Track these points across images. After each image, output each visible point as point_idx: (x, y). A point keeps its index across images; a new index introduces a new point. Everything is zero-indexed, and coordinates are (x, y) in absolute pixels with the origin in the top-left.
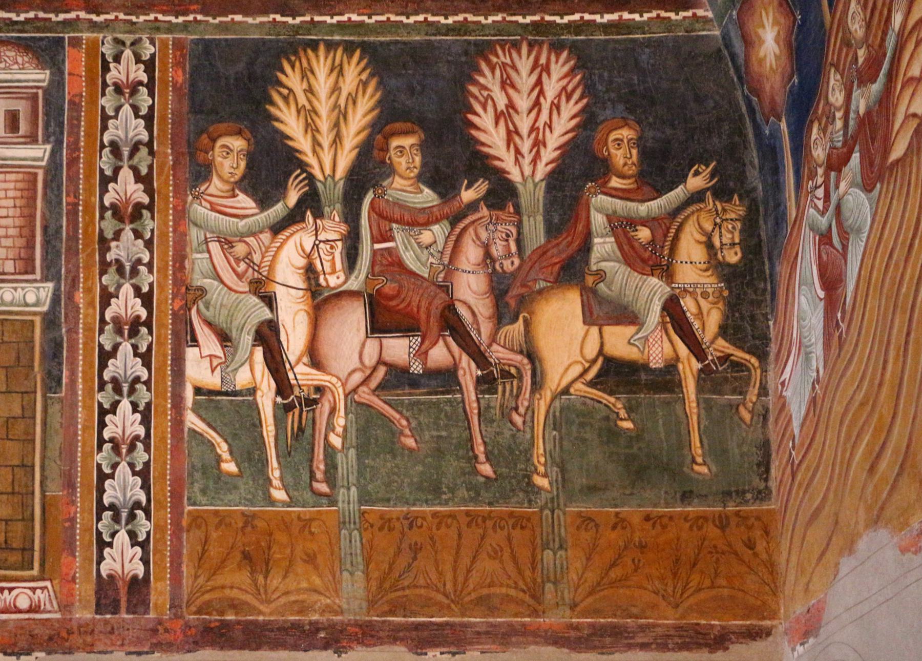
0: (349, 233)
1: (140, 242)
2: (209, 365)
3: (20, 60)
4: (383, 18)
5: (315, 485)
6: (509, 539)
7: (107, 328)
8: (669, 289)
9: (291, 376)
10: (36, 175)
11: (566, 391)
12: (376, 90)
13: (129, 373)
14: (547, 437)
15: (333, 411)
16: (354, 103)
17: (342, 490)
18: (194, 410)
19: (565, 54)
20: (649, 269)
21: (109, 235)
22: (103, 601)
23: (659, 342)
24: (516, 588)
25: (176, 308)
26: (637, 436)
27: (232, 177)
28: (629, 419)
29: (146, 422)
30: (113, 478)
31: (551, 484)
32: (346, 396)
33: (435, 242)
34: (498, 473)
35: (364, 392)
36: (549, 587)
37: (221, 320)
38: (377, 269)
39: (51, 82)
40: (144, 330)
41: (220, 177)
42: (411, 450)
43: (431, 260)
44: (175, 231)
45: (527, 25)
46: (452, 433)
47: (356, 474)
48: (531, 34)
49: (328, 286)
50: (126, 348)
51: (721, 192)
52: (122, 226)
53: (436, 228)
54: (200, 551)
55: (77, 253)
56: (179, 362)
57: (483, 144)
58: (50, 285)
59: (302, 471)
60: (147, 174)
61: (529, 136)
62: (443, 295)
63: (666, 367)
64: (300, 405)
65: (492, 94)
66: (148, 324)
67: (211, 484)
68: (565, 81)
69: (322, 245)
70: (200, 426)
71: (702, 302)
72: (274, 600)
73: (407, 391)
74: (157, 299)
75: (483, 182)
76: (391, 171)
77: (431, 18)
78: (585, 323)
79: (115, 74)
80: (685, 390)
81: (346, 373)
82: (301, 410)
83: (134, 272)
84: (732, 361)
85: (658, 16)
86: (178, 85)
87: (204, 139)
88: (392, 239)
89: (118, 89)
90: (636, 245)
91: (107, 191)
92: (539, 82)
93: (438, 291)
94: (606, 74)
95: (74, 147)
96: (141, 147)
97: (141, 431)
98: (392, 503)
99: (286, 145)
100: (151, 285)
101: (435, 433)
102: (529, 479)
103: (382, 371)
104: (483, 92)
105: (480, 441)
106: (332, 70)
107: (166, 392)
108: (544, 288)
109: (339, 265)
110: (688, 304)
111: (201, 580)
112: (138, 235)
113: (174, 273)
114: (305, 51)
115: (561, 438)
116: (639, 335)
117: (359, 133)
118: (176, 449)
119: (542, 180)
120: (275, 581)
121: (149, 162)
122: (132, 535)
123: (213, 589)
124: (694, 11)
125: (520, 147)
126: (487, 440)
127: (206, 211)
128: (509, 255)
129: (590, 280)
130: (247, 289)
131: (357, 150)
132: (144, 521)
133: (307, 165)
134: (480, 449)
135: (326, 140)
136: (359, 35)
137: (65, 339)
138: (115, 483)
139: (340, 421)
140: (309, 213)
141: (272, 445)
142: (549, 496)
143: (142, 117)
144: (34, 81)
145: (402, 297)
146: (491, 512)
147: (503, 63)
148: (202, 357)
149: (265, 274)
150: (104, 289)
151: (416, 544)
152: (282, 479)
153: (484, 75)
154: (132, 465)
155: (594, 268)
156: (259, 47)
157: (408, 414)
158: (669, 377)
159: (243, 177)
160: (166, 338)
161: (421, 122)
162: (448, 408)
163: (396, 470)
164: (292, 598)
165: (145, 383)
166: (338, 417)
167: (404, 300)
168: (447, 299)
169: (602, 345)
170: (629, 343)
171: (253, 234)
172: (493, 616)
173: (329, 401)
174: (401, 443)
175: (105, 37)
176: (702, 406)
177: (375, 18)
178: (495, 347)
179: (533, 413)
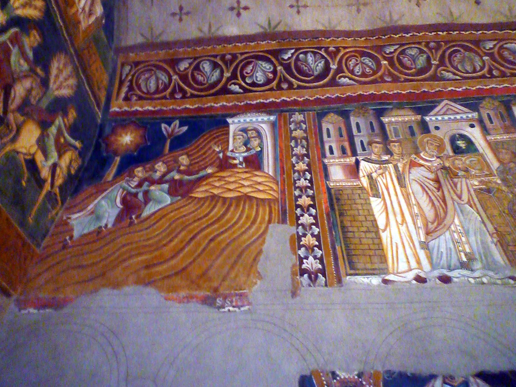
11: (18, 153)
26: (24, 190)
28: (25, 182)
76: (28, 35)
110: (58, 170)
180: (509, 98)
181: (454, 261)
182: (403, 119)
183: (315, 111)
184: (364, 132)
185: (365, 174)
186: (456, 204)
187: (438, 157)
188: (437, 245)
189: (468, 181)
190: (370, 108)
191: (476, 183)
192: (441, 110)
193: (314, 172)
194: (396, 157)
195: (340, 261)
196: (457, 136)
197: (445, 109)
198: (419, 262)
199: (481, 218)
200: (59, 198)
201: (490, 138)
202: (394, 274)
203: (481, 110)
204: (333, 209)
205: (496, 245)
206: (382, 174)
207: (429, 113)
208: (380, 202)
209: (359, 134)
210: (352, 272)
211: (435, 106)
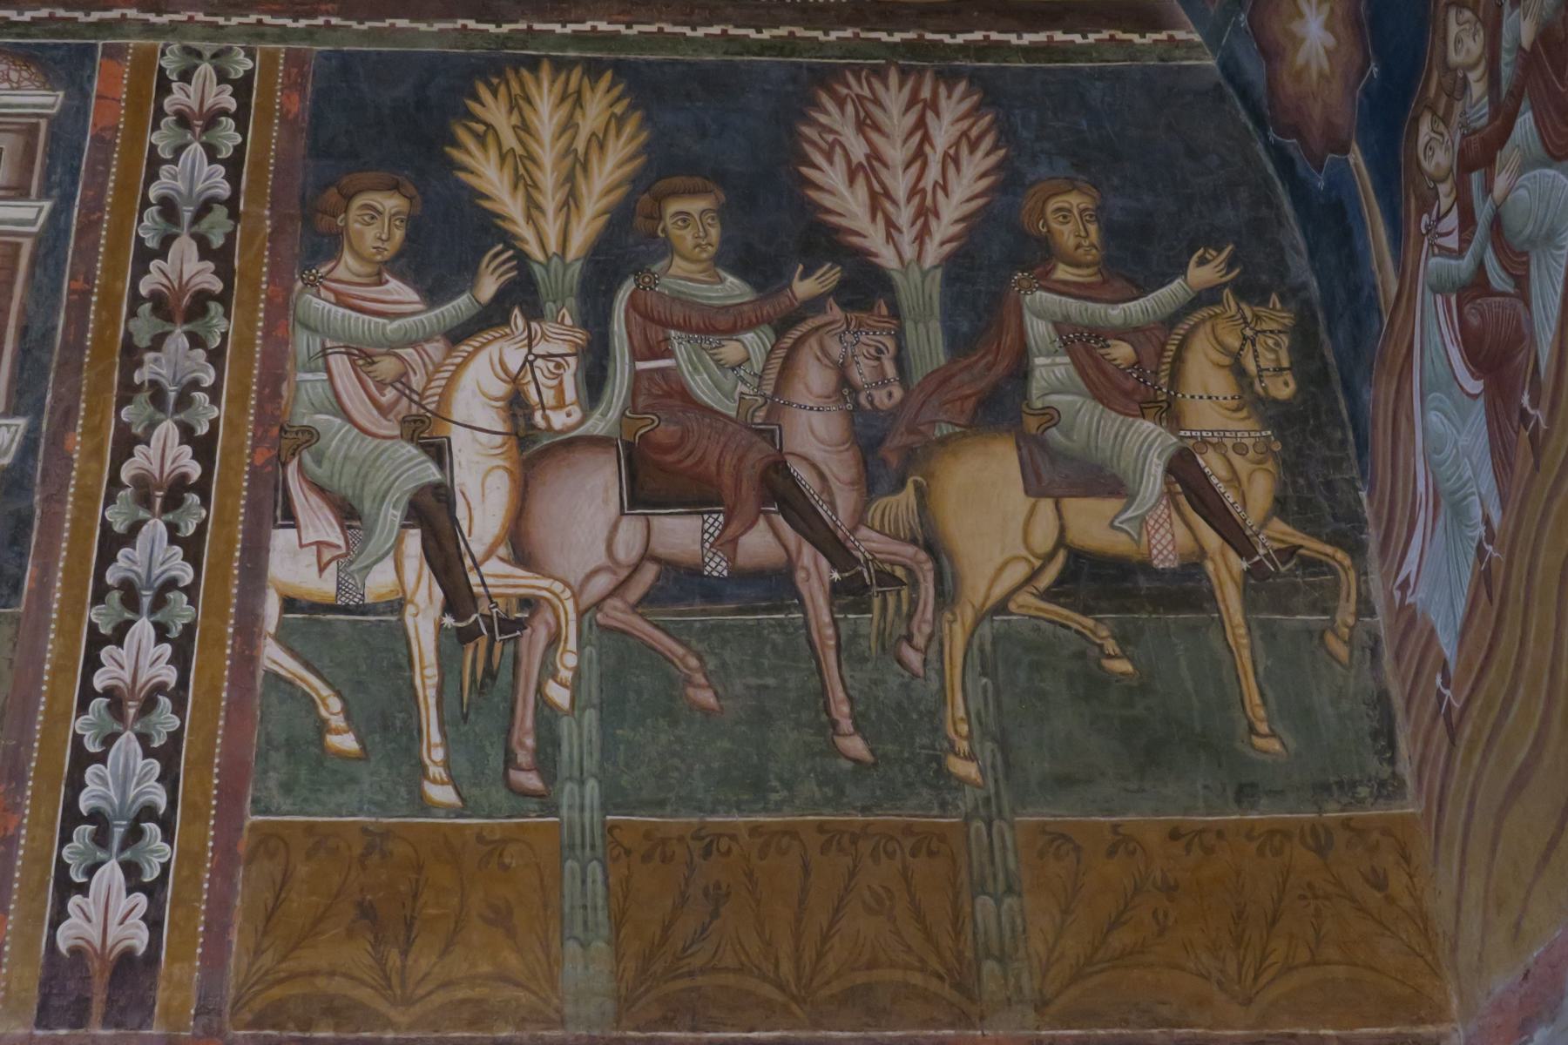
0: (590, 343)
1: (200, 354)
2: (315, 559)
3: (14, 75)
4: (653, 28)
5: (515, 775)
6: (905, 875)
7: (122, 493)
8: (1175, 440)
9: (474, 579)
10: (18, 246)
11: (1001, 607)
12: (640, 128)
13: (157, 571)
14: (969, 686)
15: (555, 640)
16: (602, 146)
17: (568, 786)
18: (277, 638)
19: (962, 86)
20: (1137, 407)
21: (142, 340)
22: (55, 1002)
23: (1167, 526)
24: (922, 970)
25: (259, 461)
27: (379, 253)
28: (1124, 655)
29: (181, 659)
30: (105, 763)
31: (982, 771)
32: (580, 615)
33: (748, 359)
34: (879, 752)
35: (615, 608)
36: (989, 966)
37: (344, 484)
38: (642, 401)
39: (64, 109)
40: (193, 499)
41: (357, 255)
42: (707, 712)
43: (741, 388)
44: (265, 337)
45: (896, 44)
46: (786, 680)
47: (596, 756)
48: (904, 57)
49: (550, 428)
50: (156, 528)
51: (1249, 290)
52: (168, 328)
53: (749, 337)
54: (270, 904)
55: (79, 369)
56: (256, 552)
57: (829, 211)
58: (21, 422)
59: (488, 748)
60: (223, 246)
61: (909, 200)
62: (764, 445)
63: (1183, 566)
64: (490, 630)
65: (842, 139)
66: (202, 488)
67: (303, 773)
68: (965, 124)
69: (539, 362)
70: (288, 665)
71: (1237, 460)
72: (423, 997)
73: (698, 607)
74: (223, 448)
75: (831, 268)
76: (667, 249)
77: (732, 31)
78: (1027, 492)
79: (179, 97)
80: (1222, 607)
81: (581, 576)
82: (492, 639)
83: (184, 401)
84: (1302, 557)
85: (1112, 37)
86: (291, 116)
87: (332, 195)
88: (669, 354)
89: (183, 120)
90: (1110, 368)
91: (147, 272)
92: (921, 123)
93: (756, 438)
94: (1034, 116)
95: (94, 206)
96: (216, 206)
97: (170, 676)
98: (668, 809)
99: (479, 207)
100: (214, 424)
101: (753, 681)
102: (939, 764)
103: (650, 572)
104: (825, 136)
105: (840, 694)
106: (563, 99)
107: (227, 604)
108: (949, 437)
109: (570, 395)
110: (1212, 464)
111: (267, 960)
112: (196, 341)
113: (260, 405)
114: (517, 72)
115: (997, 692)
116: (1129, 514)
117: (608, 192)
118: (238, 706)
119: (936, 267)
120: (423, 961)
121: (229, 229)
122: (131, 871)
123: (292, 977)
124: (1170, 32)
125: (894, 218)
126: (852, 693)
127: (328, 306)
128: (883, 382)
129: (1032, 424)
130: (397, 432)
131: (607, 216)
132: (159, 843)
133: (515, 237)
134: (842, 710)
135: (550, 201)
136: (610, 50)
137: (38, 512)
138: (107, 772)
139: (568, 660)
140: (516, 311)
141: (432, 701)
142: (980, 793)
143: (222, 162)
144: (35, 106)
145: (689, 447)
146: (869, 824)
147: (857, 95)
148: (301, 546)
149: (432, 407)
150: (123, 429)
151: (718, 886)
152: (447, 764)
153: (826, 112)
154: (144, 739)
155: (1038, 404)
156: (433, 66)
157: (700, 647)
158: (1190, 584)
159: (399, 255)
160: (235, 514)
161: (719, 177)
162: (777, 638)
163: (677, 747)
164: (460, 994)
165: (186, 590)
166: (565, 651)
167: (691, 453)
168: (771, 450)
169: (1062, 530)
170: (1112, 525)
171: (413, 344)
172: (878, 1027)
173: (548, 624)
174: (688, 697)
175: (166, 45)
176: (1257, 633)
177: (637, 29)
178: (864, 532)
179: (942, 645)
200: (1314, 546)
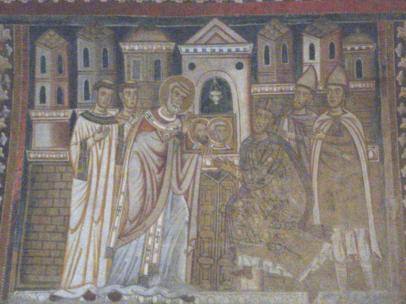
180: (305, 21)
181: (134, 275)
182: (150, 47)
183: (28, 23)
184: (93, 67)
185: (79, 140)
186: (171, 193)
187: (179, 117)
188: (124, 252)
189: (200, 159)
190: (106, 25)
191: (208, 163)
192: (205, 35)
193: (14, 133)
194: (126, 113)
195: (13, 272)
196: (215, 81)
197: (212, 33)
198: (95, 276)
199: (190, 219)
201: (256, 89)
202: (64, 289)
203: (260, 41)
204: (24, 196)
205: (188, 255)
206: (100, 141)
207: (188, 39)
208: (84, 188)
209: (85, 69)
210: (22, 286)
211: (198, 29)
